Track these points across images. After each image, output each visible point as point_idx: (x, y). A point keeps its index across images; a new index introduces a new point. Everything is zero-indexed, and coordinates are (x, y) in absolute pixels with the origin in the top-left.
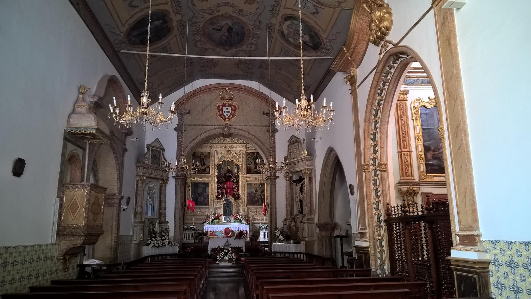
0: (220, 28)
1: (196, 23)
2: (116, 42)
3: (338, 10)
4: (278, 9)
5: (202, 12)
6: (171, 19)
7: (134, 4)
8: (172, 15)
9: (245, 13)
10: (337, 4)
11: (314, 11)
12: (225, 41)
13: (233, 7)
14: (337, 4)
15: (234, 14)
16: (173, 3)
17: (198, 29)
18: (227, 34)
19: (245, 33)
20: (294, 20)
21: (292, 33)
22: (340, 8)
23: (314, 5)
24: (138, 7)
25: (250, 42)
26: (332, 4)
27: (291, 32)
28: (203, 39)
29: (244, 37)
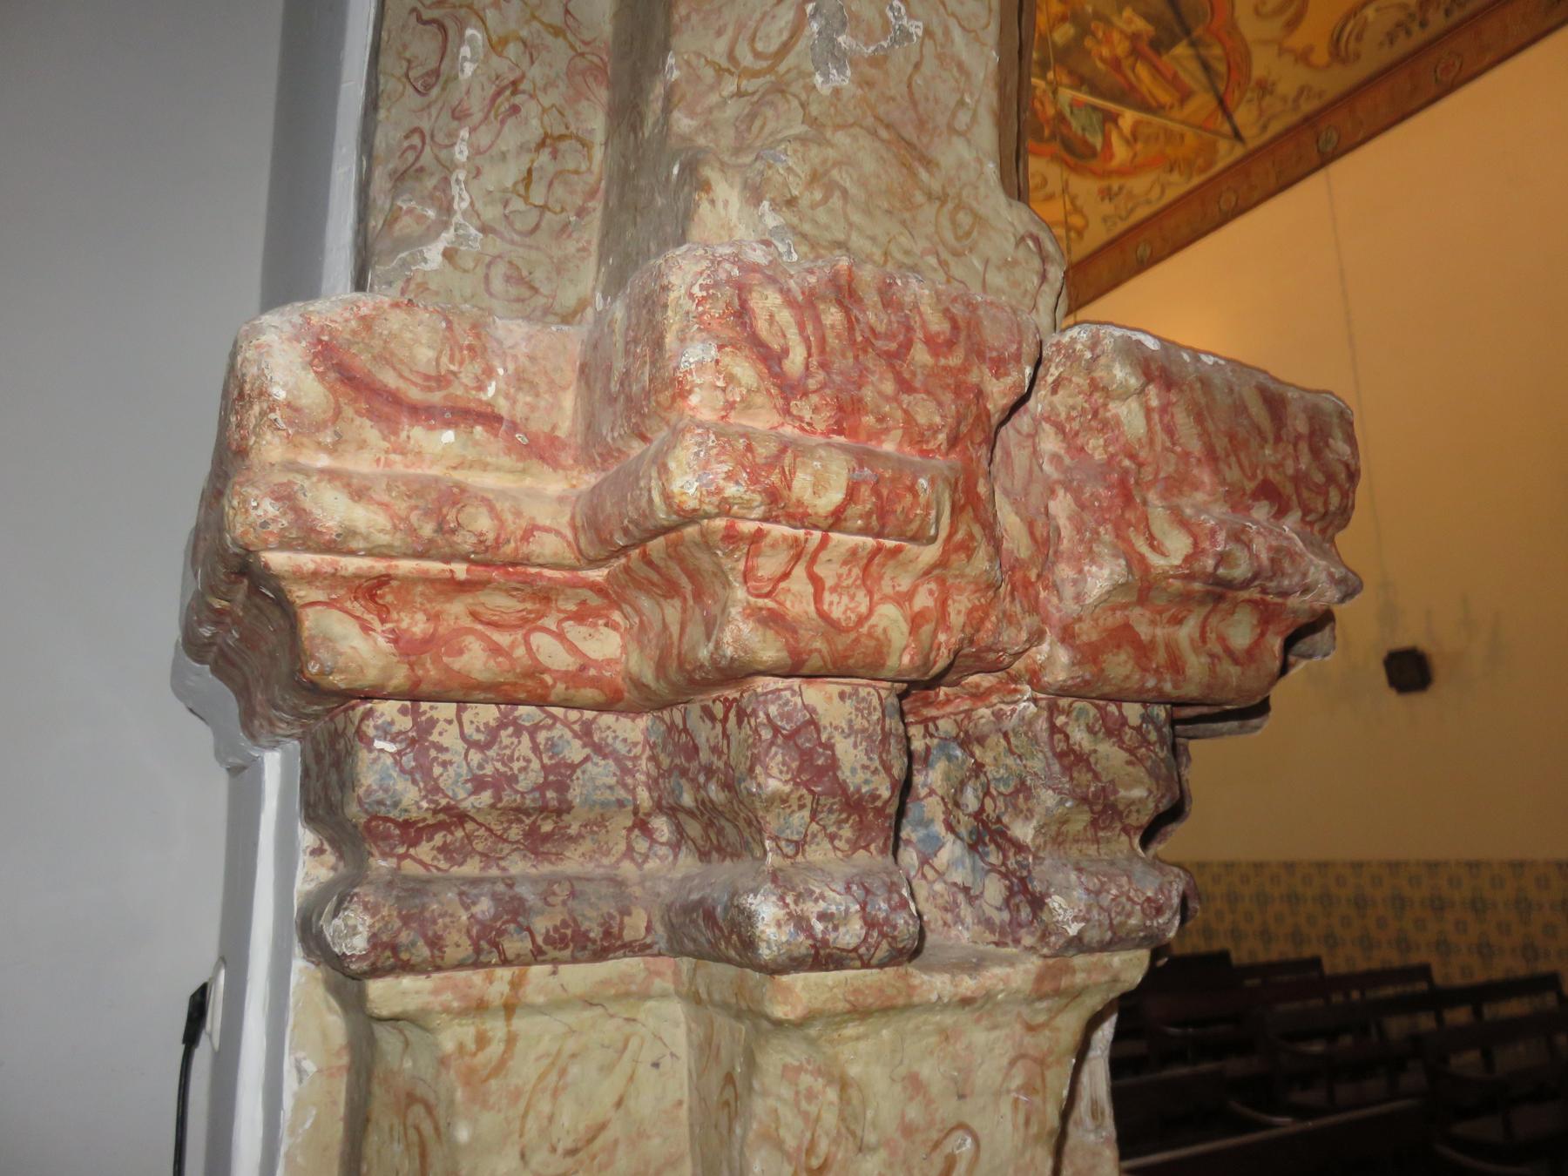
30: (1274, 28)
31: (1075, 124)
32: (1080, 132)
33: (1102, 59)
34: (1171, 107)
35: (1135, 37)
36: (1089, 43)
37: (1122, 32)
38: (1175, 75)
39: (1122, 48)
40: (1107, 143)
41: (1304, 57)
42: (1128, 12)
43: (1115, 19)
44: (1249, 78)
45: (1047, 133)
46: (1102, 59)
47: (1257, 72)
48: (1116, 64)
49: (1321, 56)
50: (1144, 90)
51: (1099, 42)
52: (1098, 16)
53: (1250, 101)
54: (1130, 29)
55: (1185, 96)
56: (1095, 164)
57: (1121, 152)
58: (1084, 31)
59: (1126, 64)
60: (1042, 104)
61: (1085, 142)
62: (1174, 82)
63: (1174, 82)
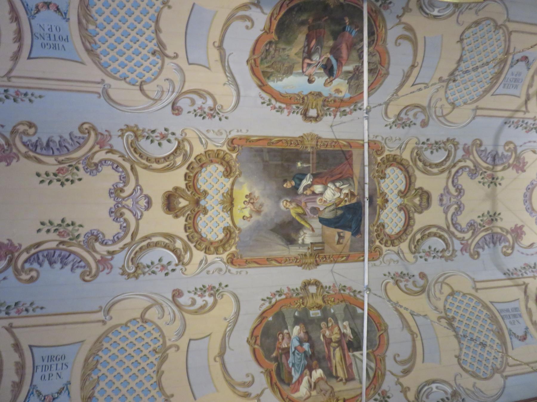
3: (512, 26)
4: (531, 122)
7: (520, 333)
10: (501, 31)
11: (522, 64)
16: (525, 275)
22: (507, 24)
23: (511, 66)
26: (503, 38)
30: (398, 369)
31: (291, 359)
32: (290, 365)
33: (324, 336)
34: (341, 380)
35: (343, 335)
36: (323, 324)
37: (340, 329)
38: (351, 364)
39: (335, 337)
40: (299, 381)
41: (405, 391)
42: (346, 323)
43: (340, 323)
44: (380, 388)
45: (274, 355)
46: (324, 336)
47: (385, 387)
48: (329, 341)
49: (411, 395)
50: (334, 361)
51: (328, 327)
52: (334, 317)
53: (376, 400)
54: (343, 331)
55: (350, 379)
56: (285, 389)
57: (303, 390)
58: (324, 318)
59: (333, 345)
60: (283, 339)
61: (290, 373)
62: (348, 368)
63: (348, 368)
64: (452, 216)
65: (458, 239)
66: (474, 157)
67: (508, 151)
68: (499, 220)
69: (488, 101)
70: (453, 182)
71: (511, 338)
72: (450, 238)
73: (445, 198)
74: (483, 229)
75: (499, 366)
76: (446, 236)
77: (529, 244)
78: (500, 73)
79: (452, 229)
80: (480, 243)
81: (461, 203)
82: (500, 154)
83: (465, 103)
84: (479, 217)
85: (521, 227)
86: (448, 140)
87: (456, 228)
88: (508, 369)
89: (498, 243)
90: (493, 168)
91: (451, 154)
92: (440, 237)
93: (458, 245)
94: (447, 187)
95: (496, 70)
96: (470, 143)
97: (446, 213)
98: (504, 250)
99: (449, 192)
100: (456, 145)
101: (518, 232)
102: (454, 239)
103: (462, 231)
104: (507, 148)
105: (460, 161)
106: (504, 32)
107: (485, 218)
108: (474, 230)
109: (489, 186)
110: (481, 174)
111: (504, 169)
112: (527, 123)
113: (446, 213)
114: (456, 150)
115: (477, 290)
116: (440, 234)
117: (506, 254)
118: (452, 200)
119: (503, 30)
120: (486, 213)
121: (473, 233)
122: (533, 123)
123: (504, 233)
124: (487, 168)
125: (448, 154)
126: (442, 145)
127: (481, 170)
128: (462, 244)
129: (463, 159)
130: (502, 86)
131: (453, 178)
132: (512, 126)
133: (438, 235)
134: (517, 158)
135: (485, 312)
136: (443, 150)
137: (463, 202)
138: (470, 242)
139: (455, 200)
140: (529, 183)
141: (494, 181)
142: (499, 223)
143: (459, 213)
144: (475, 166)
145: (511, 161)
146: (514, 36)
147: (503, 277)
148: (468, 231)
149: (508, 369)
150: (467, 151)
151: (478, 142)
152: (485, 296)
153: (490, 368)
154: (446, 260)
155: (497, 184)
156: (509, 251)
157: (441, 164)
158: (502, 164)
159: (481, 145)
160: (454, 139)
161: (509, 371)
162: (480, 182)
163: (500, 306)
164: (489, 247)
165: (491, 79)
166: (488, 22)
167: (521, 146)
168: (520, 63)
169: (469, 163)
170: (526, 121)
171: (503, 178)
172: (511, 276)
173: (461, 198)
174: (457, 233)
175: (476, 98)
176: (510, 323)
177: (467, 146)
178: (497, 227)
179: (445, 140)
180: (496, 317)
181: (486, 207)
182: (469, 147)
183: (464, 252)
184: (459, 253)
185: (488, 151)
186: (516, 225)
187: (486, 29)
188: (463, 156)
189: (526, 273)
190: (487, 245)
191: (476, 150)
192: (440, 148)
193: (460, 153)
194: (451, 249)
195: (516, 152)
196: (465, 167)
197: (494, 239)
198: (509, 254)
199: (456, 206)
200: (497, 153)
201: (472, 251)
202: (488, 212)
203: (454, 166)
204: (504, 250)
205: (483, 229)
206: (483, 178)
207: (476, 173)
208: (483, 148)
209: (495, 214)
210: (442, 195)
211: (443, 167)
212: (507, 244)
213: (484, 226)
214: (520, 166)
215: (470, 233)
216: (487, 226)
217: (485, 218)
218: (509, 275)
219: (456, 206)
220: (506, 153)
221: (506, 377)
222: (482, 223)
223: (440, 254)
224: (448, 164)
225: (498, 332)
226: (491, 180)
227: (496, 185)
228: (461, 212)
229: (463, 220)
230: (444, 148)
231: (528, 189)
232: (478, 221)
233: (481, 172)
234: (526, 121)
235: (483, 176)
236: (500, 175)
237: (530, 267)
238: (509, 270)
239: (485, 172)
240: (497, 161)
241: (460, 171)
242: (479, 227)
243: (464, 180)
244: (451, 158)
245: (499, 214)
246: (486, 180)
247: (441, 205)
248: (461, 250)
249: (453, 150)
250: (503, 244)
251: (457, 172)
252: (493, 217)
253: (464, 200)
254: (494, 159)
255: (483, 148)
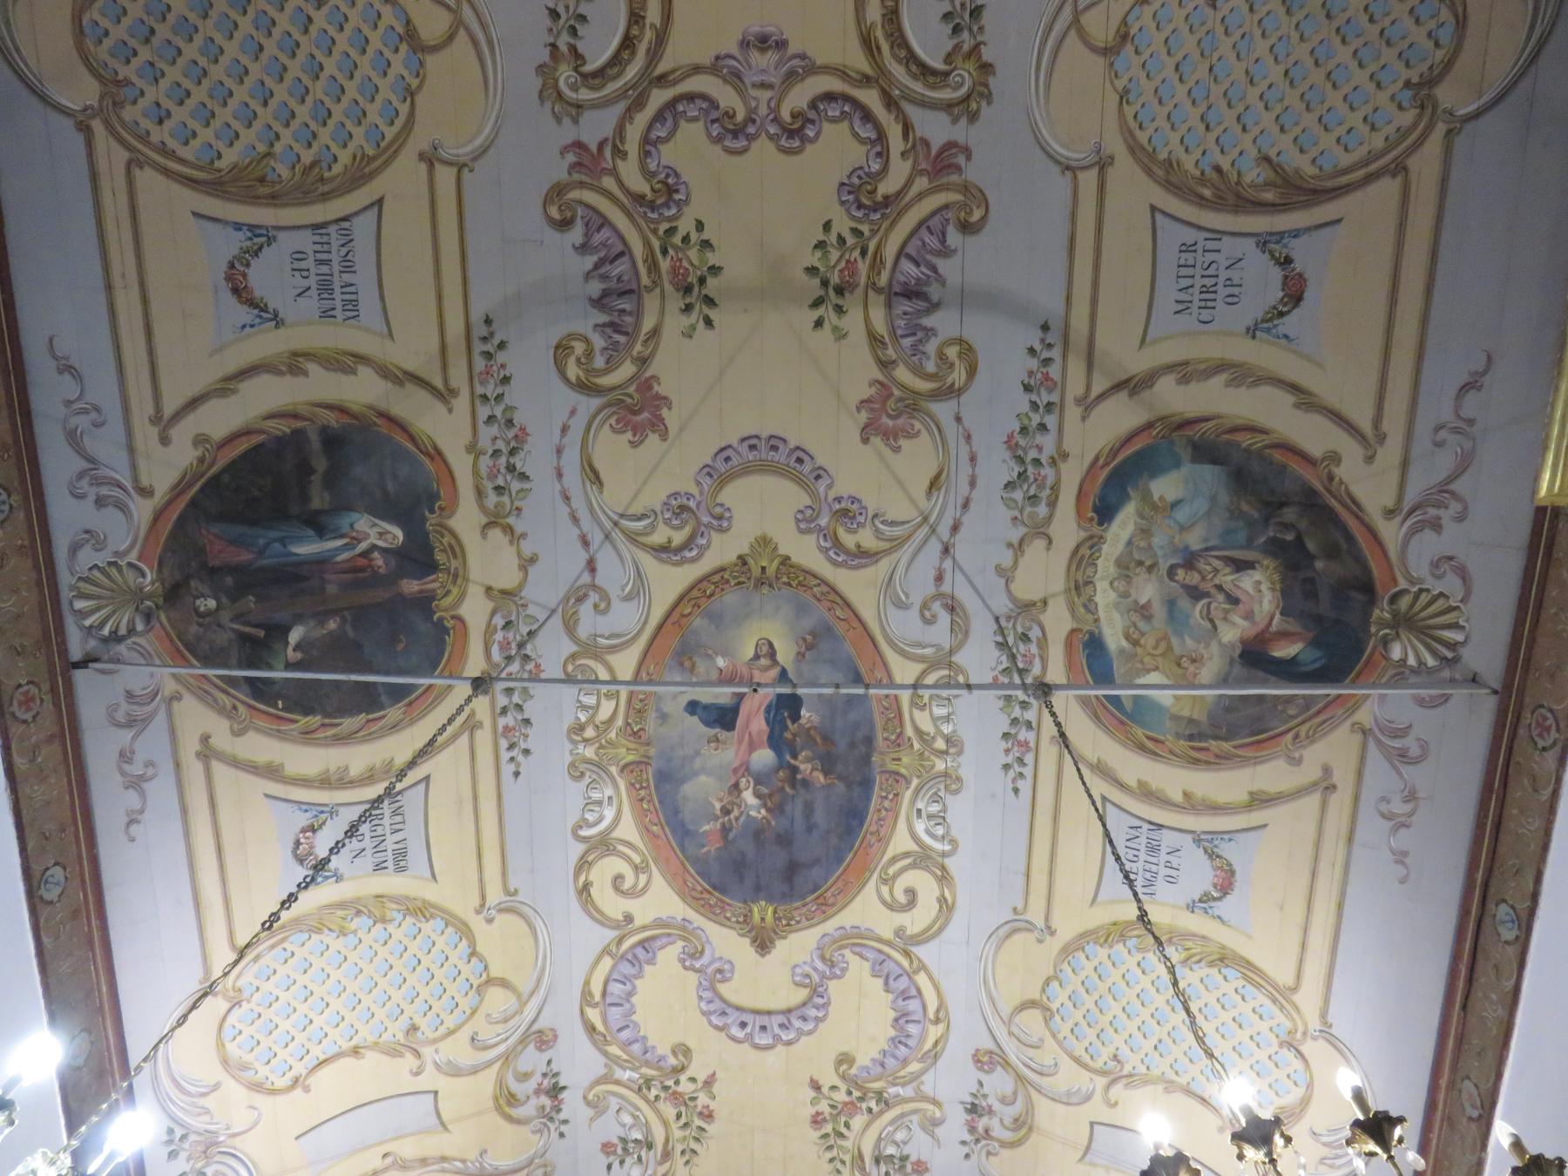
0: (722, 695)
1: (597, 657)
2: (87, 557)
4: (1048, 442)
5: (633, 538)
6: (457, 549)
8: (465, 520)
9: (866, 539)
12: (758, 833)
13: (799, 481)
14: (1408, 118)
15: (806, 552)
16: (483, 412)
17: (607, 709)
18: (764, 757)
19: (869, 740)
20: (1156, 471)
21: (1159, 611)
23: (1264, 242)
24: (278, 322)
25: (901, 842)
27: (1144, 611)
28: (628, 830)
29: (867, 784)
64: (704, 97)
65: (620, 131)
66: (920, 196)
67: (941, 356)
68: (686, 321)
69: (1132, 190)
70: (830, 97)
71: (238, 227)
72: (622, 94)
73: (771, 57)
74: (656, 244)
75: (128, 113)
76: (632, 72)
77: (598, 465)
78: (1242, 202)
79: (659, 97)
80: (605, 233)
81: (751, 138)
82: (927, 321)
83: (1124, 96)
84: (700, 226)
85: (658, 425)
86: (986, 68)
87: (659, 117)
88: (122, 156)
89: (603, 318)
90: (879, 291)
91: (933, 87)
92: (628, 43)
93: (596, 127)
94: (812, 69)
95: (1253, 174)
96: (973, 172)
97: (715, 67)
98: (579, 348)
99: (791, 77)
100: (964, 109)
101: (640, 411)
102: (620, 107)
103: (648, 144)
104: (952, 352)
105: (907, 128)
106: (1403, 133)
107: (693, 254)
108: (652, 206)
109: (812, 271)
110: (856, 232)
111: (874, 340)
112: (1042, 427)
113: (715, 67)
114: (948, 107)
115: (430, 159)
116: (640, 38)
117: (561, 350)
118: (765, 95)
119: (1415, 125)
120: (712, 259)
121: (639, 199)
122: (1044, 459)
123: (638, 348)
124: (877, 263)
125: (934, 72)
126: (967, 40)
127: (874, 232)
128: (601, 146)
129: (916, 145)
130: (1190, 235)
131: (847, 98)
132: (1033, 364)
133: (635, 31)
134: (912, 405)
135: (344, 157)
136: (949, 46)
137: (755, 145)
138: (608, 183)
139: (763, 110)
140: (821, 460)
141: (832, 292)
142: (675, 322)
143: (716, 130)
144: (887, 201)
145: (902, 374)
146: (1388, 188)
147: (477, 316)
148: (648, 175)
149: (122, 156)
150: (943, 163)
151: (977, 215)
152: (402, 179)
153: (124, 72)
154: (541, 69)
155: (820, 311)
156: (573, 371)
157: (899, 39)
158: (893, 331)
159: (966, 228)
160: (988, 98)
161: (112, 156)
162: (827, 226)
163: (363, 227)
164: (588, 276)
165: (1218, 169)
166: (1446, 35)
167: (958, 419)
168: (1277, 274)
169: (899, 170)
170: (1051, 421)
171: (840, 335)
172: (478, 347)
173: (771, 137)
174: (642, 118)
175: (1143, 137)
176: (299, 256)
177: (961, 160)
178: (662, 312)
179: (987, 54)
180: (325, 197)
181: (736, 260)
182: (959, 169)
183: (571, 158)
184: (568, 133)
185: (941, 264)
186: (666, 401)
187: (1419, 35)
188: (926, 143)
189: (491, 419)
190: (597, 266)
191: (946, 207)
192: (957, 30)
193: (935, 128)
194: (585, 95)
195: (935, 395)
196: (884, 155)
197: (617, 300)
198: (562, 373)
199: (740, 116)
200: (934, 307)
201: (575, 194)
202: (715, 270)
203: (890, 103)
204: (579, 348)
205: (656, 244)
206: (841, 240)
207: (860, 206)
208: (954, 237)
209: (710, 301)
210: (781, 45)
211: (885, 47)
212: (599, 362)
213: (665, 252)
214: (888, 416)
215: (640, 185)
216: (665, 264)
217: (693, 254)
218: (485, 341)
219: (740, 116)
220: (931, 347)
221: (84, 129)
222: (677, 240)
223: (563, 41)
224: (898, 71)
225: (262, 180)
226: (835, 279)
227: (817, 303)
228: (718, 140)
229: (688, 150)
230: (957, 47)
231: (800, 455)
232: (685, 225)
233: (865, 228)
234: (1051, 421)
235: (850, 241)
236: (853, 320)
237: (512, 452)
238: (502, 345)
239: (864, 253)
240: (904, 306)
241: (867, 132)
242: (664, 226)
243: (837, 149)
244: (918, 87)
245: (709, 322)
246: (834, 255)
247: (745, 44)
248: (579, 145)
249: (946, 95)
250: (598, 342)
251: (868, 116)
252: (697, 293)
253: (763, 148)
254: (910, 293)
255: (954, 237)
